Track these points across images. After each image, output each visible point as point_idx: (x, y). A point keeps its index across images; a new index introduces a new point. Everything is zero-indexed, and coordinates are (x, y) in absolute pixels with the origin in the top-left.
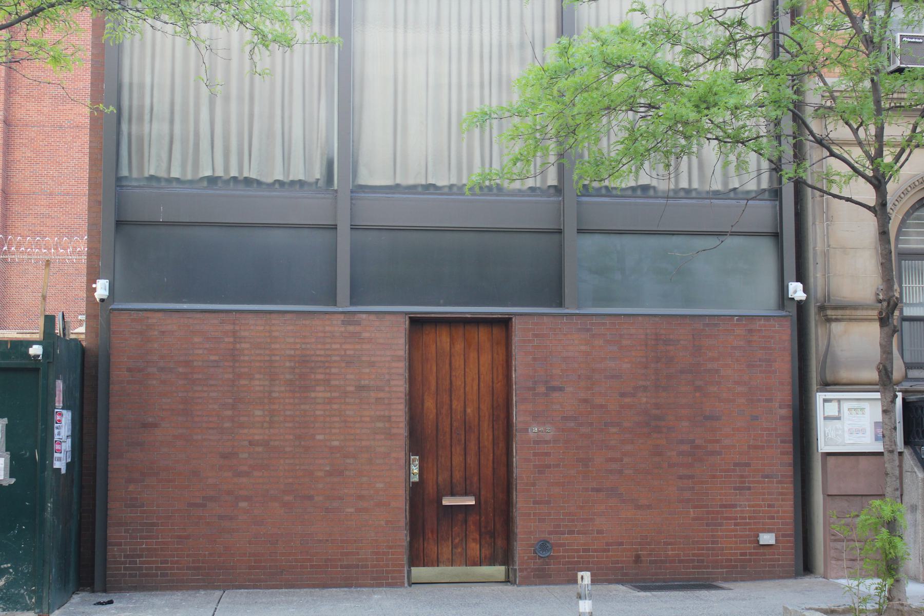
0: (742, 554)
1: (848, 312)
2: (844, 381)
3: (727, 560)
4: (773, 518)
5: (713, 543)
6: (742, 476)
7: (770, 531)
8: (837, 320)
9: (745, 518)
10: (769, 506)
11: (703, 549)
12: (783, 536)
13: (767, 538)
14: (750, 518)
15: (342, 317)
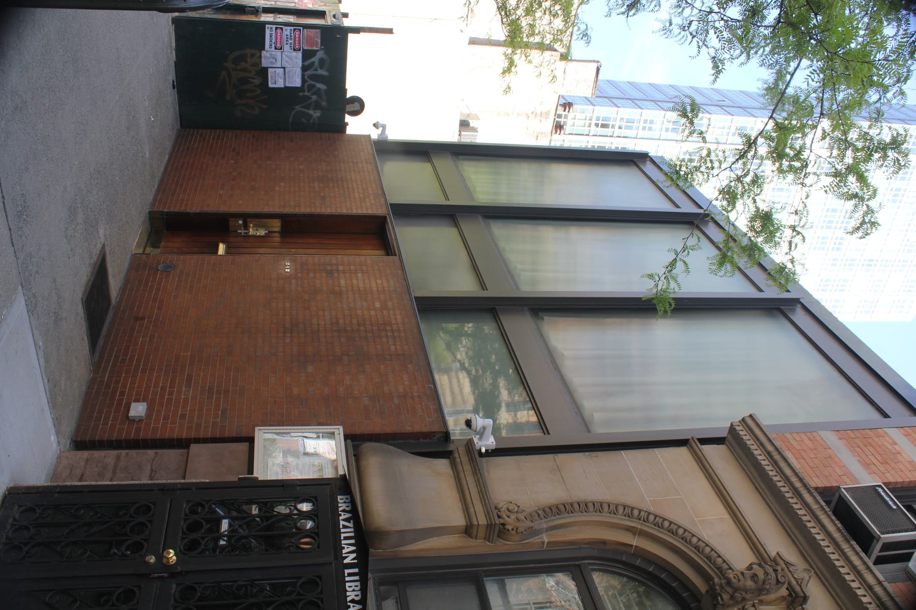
0: (122, 394)
1: (467, 467)
2: (363, 463)
3: (118, 382)
4: (166, 418)
5: (144, 371)
6: (226, 392)
7: (150, 410)
8: (453, 465)
9: (171, 393)
10: (183, 416)
11: (139, 361)
12: (138, 430)
13: (138, 409)
14: (169, 400)
15: (380, 192)
